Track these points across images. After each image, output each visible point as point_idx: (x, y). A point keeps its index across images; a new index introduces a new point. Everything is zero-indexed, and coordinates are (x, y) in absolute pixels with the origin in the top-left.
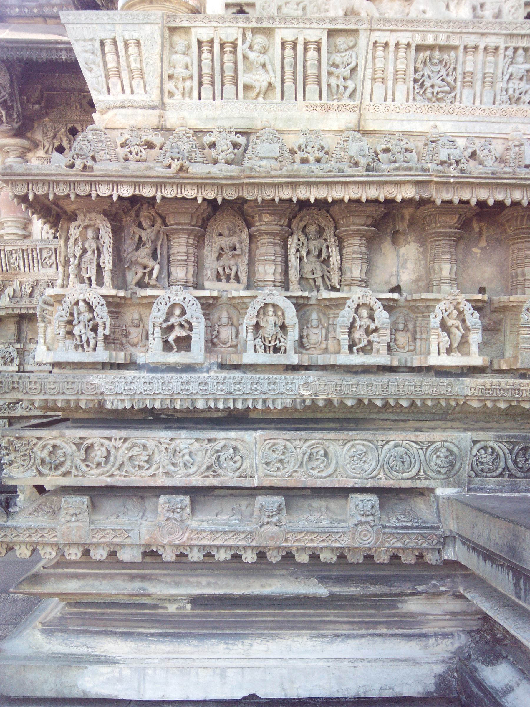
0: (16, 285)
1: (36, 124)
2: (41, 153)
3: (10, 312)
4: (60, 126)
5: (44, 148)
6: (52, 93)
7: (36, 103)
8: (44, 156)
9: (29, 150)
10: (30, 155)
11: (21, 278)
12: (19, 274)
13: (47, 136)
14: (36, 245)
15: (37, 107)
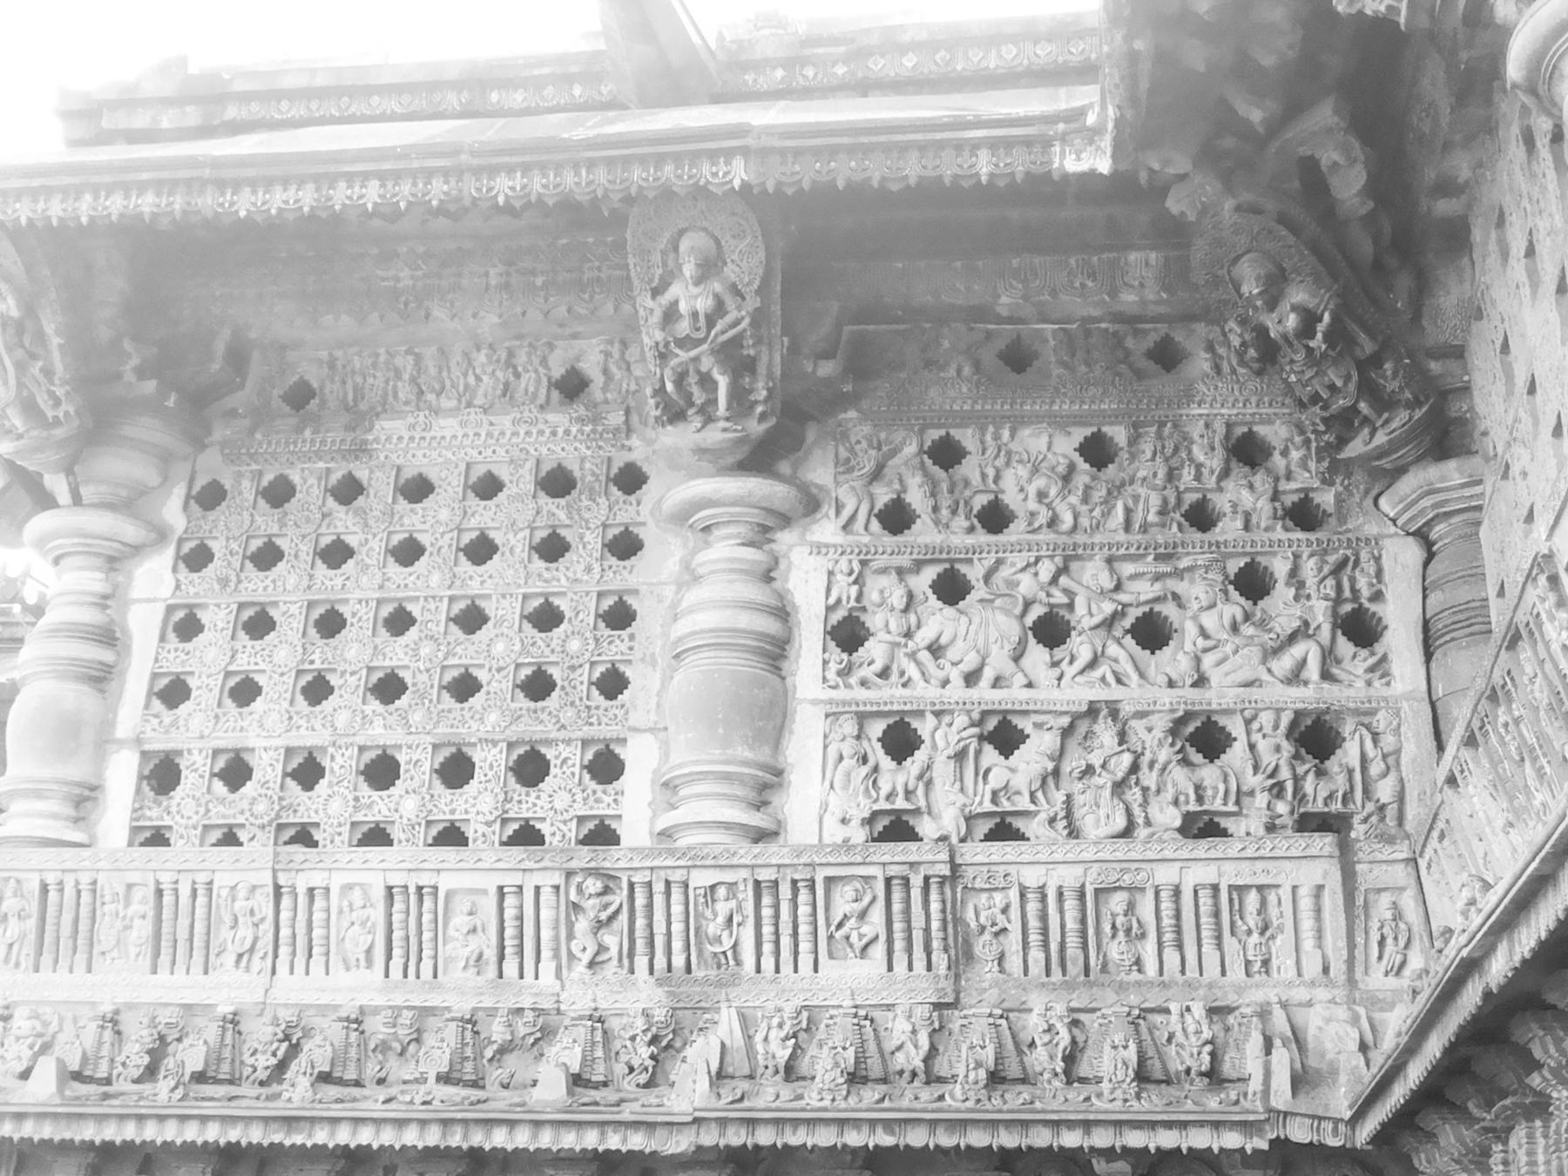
0: (727, 1026)
1: (811, 433)
2: (826, 530)
3: (709, 1138)
4: (898, 436)
5: (838, 513)
6: (871, 327)
7: (828, 355)
8: (840, 539)
9: (785, 520)
10: (785, 538)
11: (744, 996)
12: (735, 980)
13: (850, 470)
14: (812, 865)
15: (827, 369)
